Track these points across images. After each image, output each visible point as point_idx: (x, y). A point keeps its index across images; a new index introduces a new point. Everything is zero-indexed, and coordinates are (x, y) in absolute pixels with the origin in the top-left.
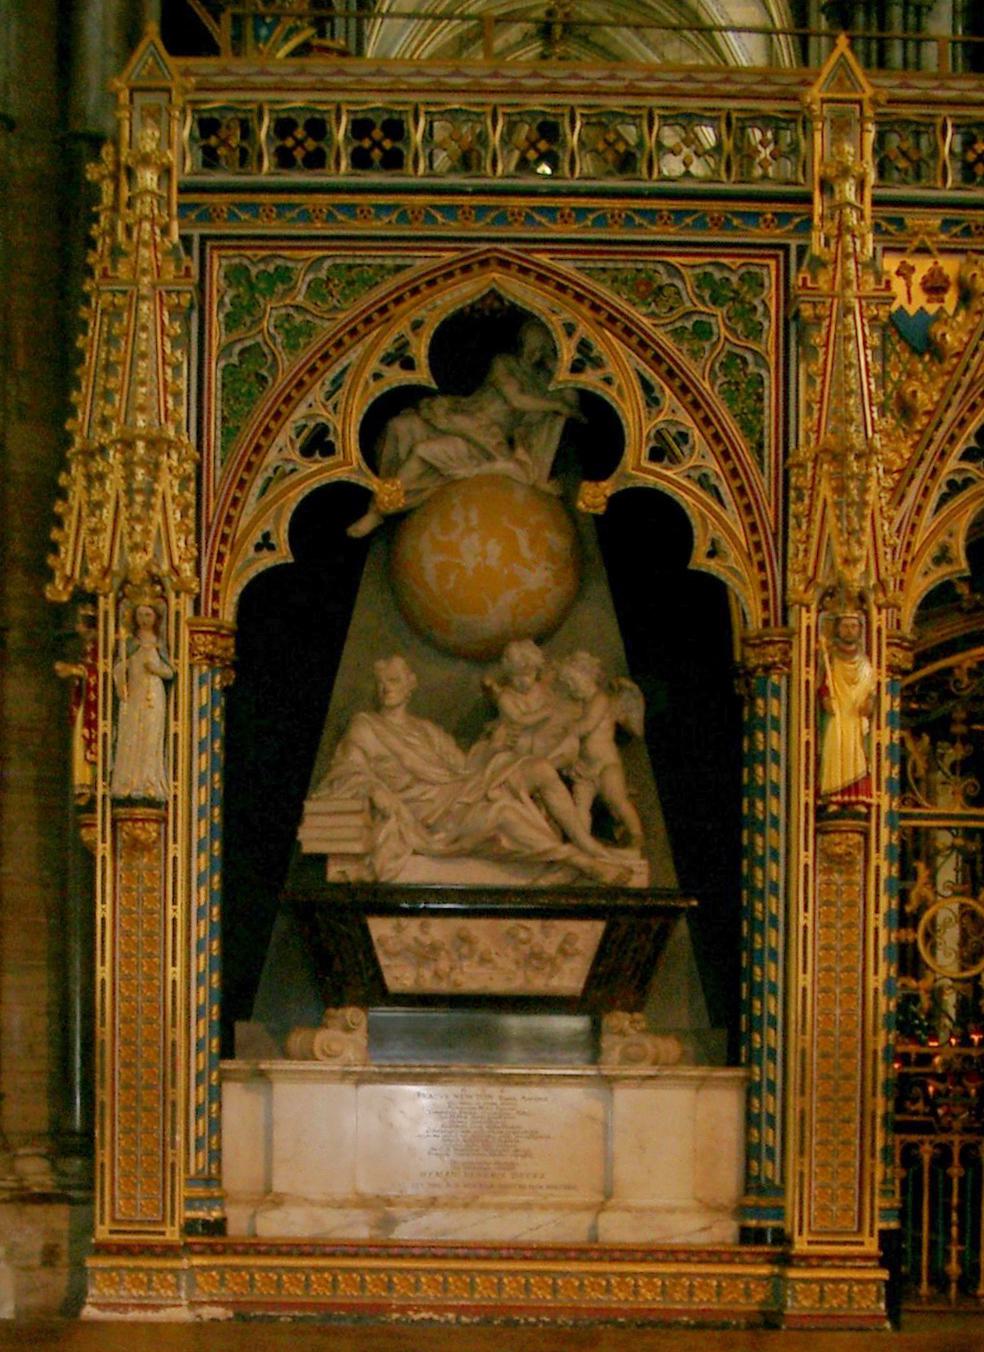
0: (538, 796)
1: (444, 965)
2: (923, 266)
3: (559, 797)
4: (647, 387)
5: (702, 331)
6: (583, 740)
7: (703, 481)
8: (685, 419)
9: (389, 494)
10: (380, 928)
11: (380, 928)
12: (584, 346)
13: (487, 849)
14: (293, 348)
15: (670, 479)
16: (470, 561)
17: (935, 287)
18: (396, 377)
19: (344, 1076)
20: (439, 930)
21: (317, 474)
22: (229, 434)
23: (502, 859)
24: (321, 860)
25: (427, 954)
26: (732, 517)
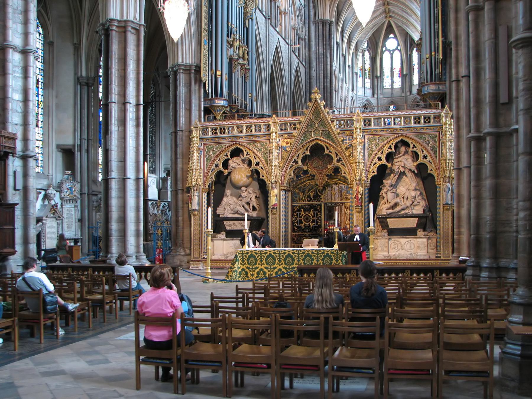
0: (243, 207)
1: (232, 227)
2: (286, 140)
3: (247, 207)
4: (255, 157)
5: (261, 150)
6: (251, 199)
7: (261, 168)
8: (259, 161)
9: (226, 172)
10: (225, 222)
11: (225, 222)
12: (247, 153)
13: (237, 213)
14: (214, 155)
15: (258, 168)
16: (237, 178)
17: (287, 143)
18: (226, 157)
19: (221, 240)
20: (231, 222)
21: (216, 170)
22: (207, 166)
23: (239, 214)
24: (219, 215)
25: (230, 226)
26: (264, 172)
